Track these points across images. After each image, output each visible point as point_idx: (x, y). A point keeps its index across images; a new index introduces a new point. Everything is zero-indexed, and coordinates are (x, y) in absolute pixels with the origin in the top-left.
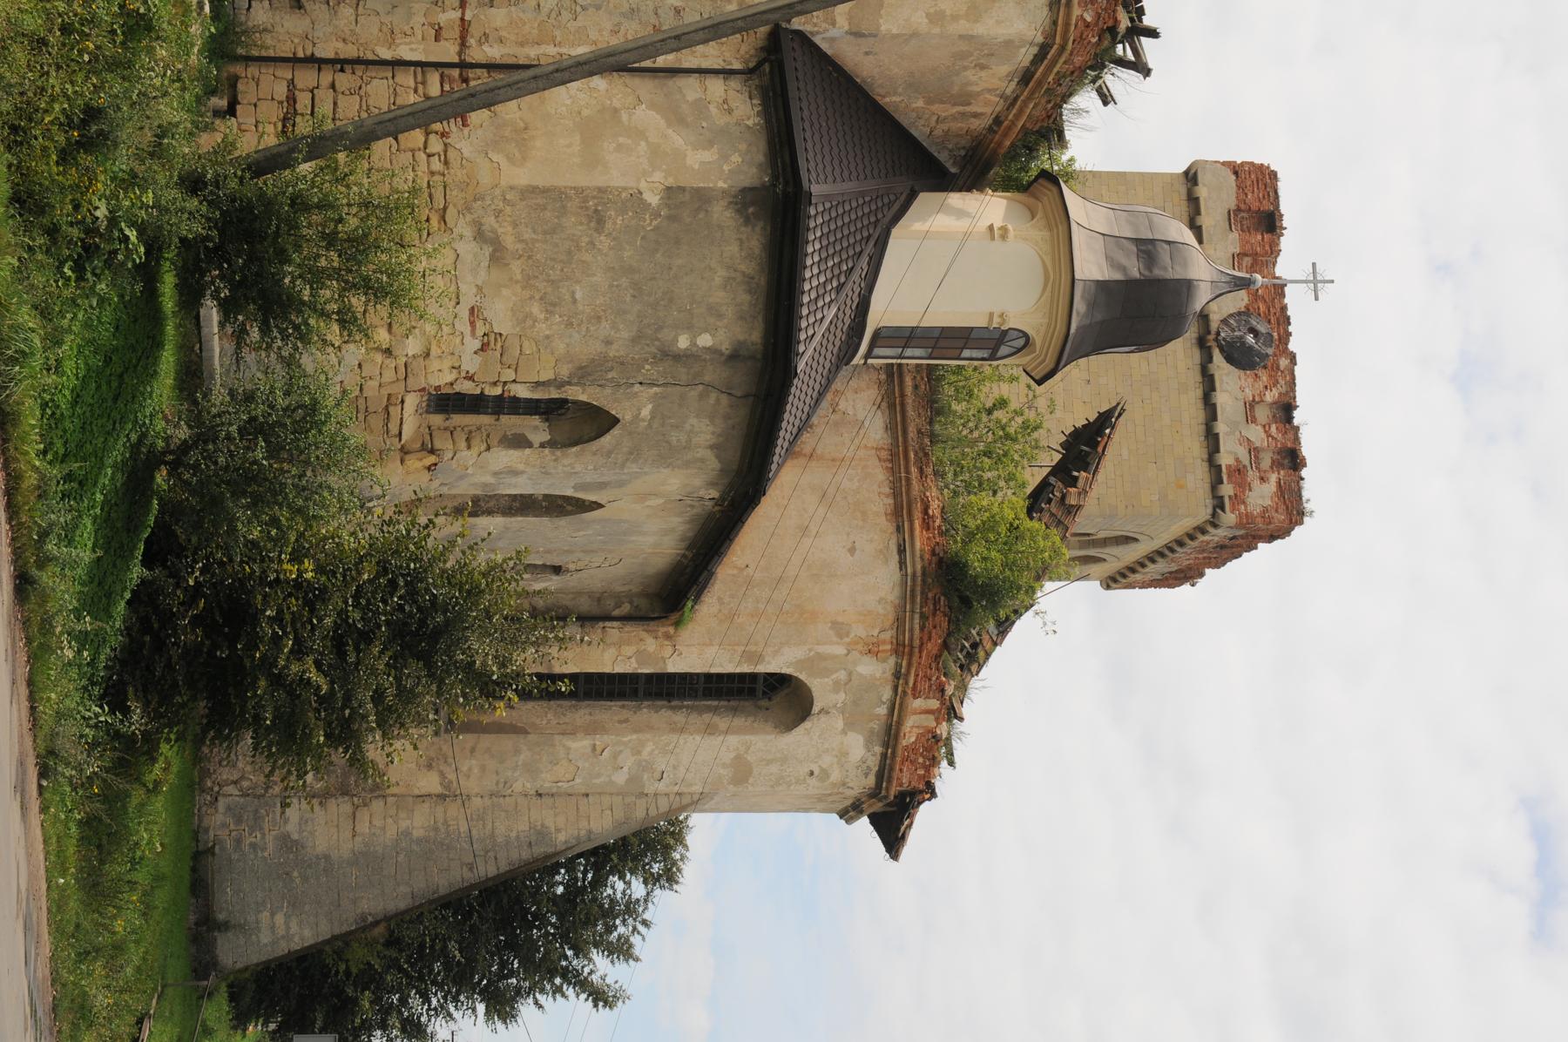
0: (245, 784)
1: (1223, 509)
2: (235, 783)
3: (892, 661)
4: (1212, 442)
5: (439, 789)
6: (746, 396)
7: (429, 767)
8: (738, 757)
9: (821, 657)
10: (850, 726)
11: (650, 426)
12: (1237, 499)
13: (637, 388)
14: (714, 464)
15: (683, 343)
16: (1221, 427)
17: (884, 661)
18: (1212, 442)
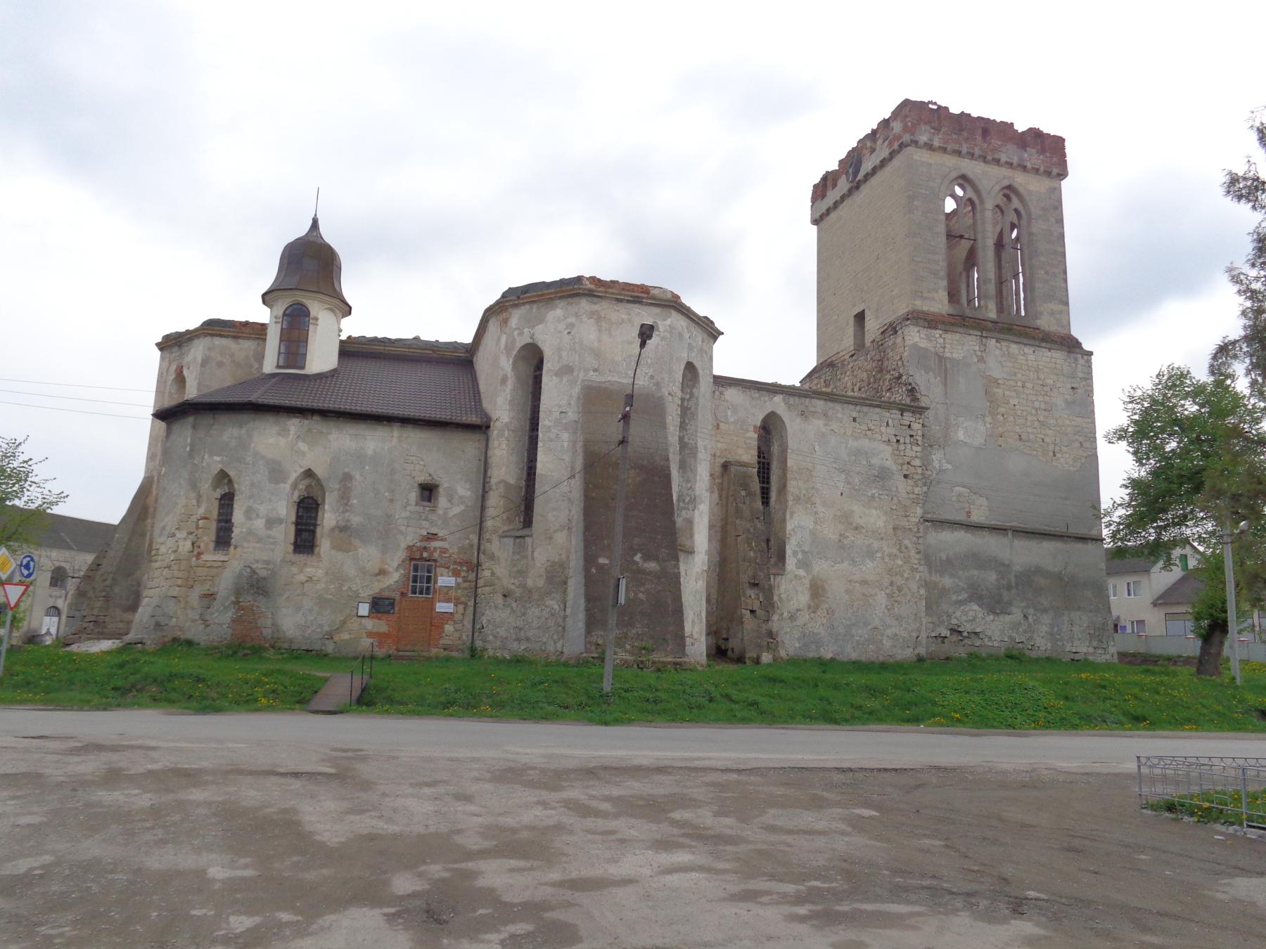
0: (555, 637)
1: (902, 143)
2: (555, 643)
3: (510, 310)
4: (884, 163)
5: (565, 531)
6: (214, 418)
7: (550, 538)
8: (556, 375)
9: (506, 347)
10: (541, 321)
11: (227, 456)
12: (898, 137)
13: (204, 464)
14: (251, 425)
15: (188, 449)
16: (878, 162)
17: (510, 314)
18: (884, 163)
